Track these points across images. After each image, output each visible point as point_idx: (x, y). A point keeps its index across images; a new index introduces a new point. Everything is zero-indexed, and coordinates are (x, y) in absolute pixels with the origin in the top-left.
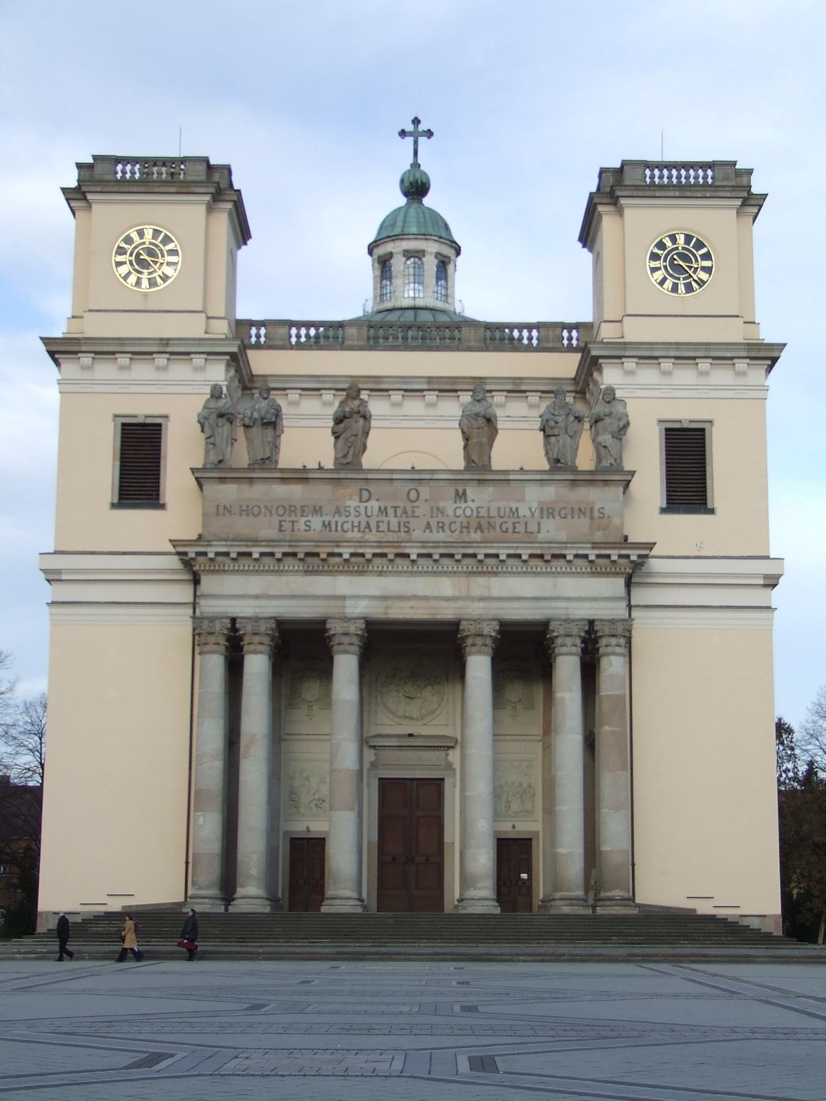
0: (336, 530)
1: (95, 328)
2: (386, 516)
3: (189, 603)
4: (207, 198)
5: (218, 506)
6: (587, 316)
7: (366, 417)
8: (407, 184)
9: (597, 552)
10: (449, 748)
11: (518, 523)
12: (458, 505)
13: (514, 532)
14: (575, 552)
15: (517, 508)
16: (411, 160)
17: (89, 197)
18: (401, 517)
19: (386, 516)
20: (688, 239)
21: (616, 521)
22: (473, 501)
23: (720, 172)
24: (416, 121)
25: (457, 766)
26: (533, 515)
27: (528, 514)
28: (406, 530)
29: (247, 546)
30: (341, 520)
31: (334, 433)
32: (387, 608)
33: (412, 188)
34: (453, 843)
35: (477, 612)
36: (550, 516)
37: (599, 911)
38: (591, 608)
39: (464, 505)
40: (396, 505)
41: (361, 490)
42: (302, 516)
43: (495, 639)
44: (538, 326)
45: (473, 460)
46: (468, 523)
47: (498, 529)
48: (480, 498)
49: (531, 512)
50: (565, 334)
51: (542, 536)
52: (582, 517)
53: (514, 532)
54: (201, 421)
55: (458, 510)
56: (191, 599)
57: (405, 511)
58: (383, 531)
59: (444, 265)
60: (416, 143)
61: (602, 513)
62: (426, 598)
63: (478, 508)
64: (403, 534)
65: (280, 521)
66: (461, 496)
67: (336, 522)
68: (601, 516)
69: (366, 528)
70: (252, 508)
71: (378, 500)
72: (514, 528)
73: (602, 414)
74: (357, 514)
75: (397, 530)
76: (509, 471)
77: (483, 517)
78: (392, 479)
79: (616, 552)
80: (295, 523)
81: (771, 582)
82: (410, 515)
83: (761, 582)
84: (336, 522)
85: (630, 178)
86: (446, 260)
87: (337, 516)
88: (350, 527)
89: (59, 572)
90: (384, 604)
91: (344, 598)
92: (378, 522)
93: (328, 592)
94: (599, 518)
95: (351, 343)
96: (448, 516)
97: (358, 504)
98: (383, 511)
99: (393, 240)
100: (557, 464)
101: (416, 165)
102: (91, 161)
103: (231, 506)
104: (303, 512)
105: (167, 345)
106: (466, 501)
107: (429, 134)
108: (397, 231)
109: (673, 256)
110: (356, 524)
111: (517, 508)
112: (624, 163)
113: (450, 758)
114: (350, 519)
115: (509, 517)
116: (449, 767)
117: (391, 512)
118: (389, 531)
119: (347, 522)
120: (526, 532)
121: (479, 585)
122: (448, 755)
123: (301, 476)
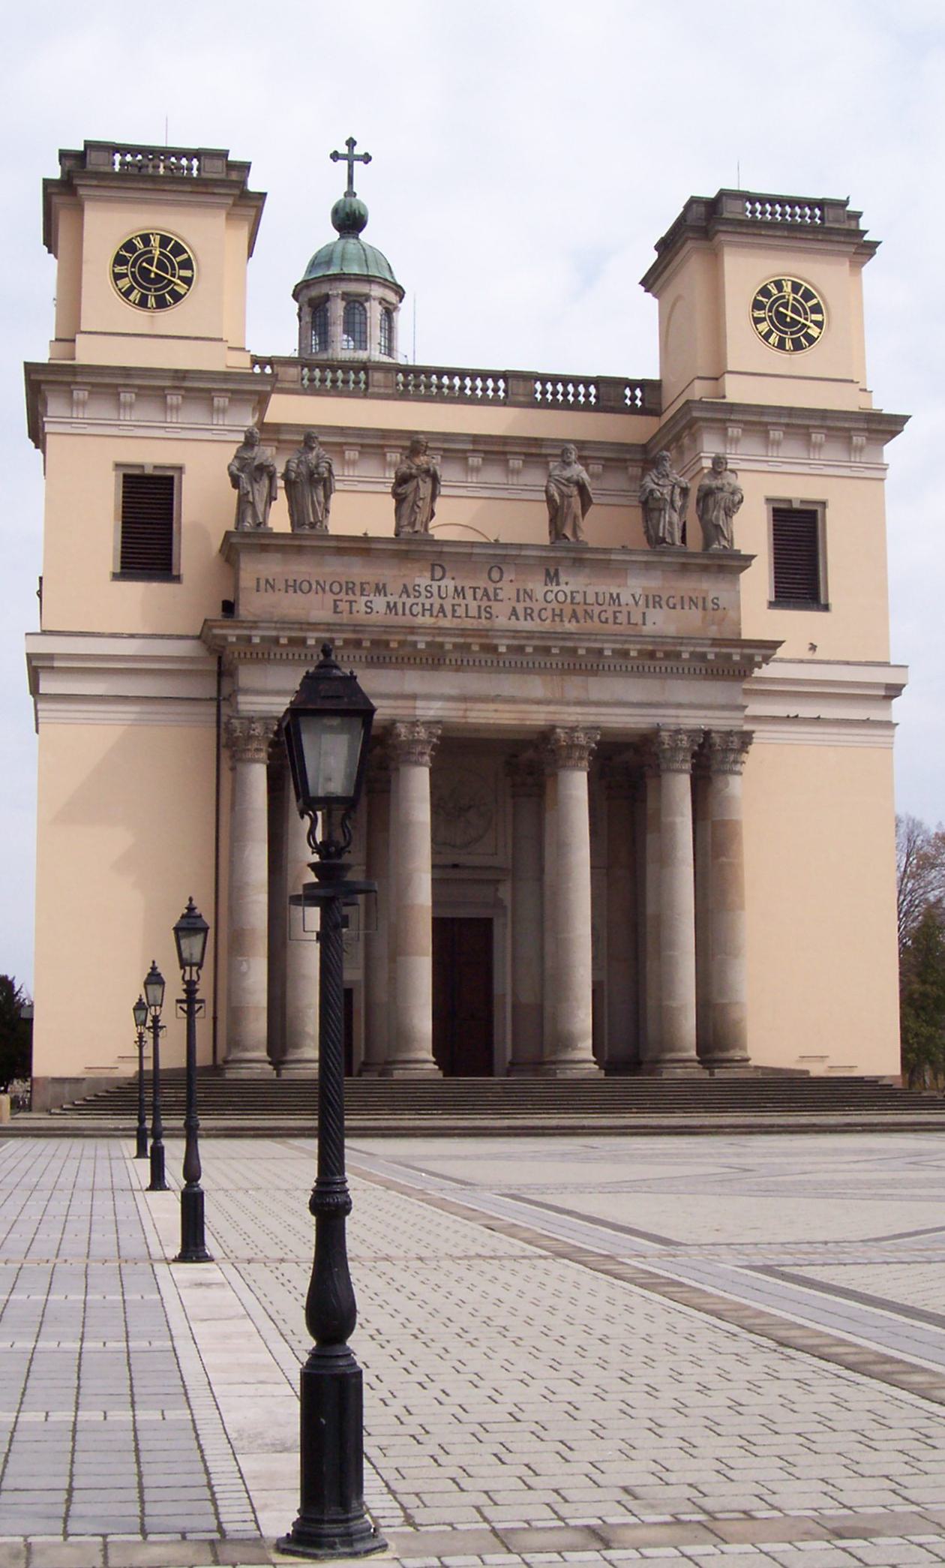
0: (404, 614)
1: (89, 353)
2: (464, 598)
3: (211, 699)
4: (230, 201)
5: (258, 579)
6: (654, 375)
7: (435, 479)
8: (342, 215)
9: (717, 650)
10: (498, 881)
11: (620, 612)
12: (549, 588)
13: (615, 623)
14: (692, 649)
15: (618, 595)
16: (346, 189)
17: (82, 191)
18: (481, 600)
19: (464, 598)
20: (796, 287)
21: (731, 614)
22: (567, 584)
23: (830, 213)
24: (351, 143)
25: (508, 903)
26: (637, 603)
27: (631, 601)
28: (488, 615)
29: (301, 629)
30: (409, 601)
31: (395, 494)
32: (466, 710)
33: (349, 220)
34: (504, 995)
35: (573, 718)
36: (657, 605)
37: (719, 1074)
38: (706, 717)
39: (556, 589)
40: (474, 585)
41: (433, 565)
42: (362, 595)
43: (592, 752)
44: (598, 381)
45: (564, 535)
46: (561, 610)
47: (596, 619)
48: (572, 583)
49: (634, 598)
50: (628, 392)
51: (648, 629)
52: (693, 607)
53: (615, 623)
54: (236, 472)
55: (550, 593)
56: (214, 694)
57: (486, 593)
58: (459, 617)
59: (389, 312)
60: (351, 167)
61: (716, 604)
62: (512, 700)
63: (572, 593)
64: (483, 621)
65: (335, 601)
66: (552, 577)
67: (404, 604)
68: (716, 607)
69: (439, 612)
70: (301, 583)
71: (453, 579)
72: (615, 618)
73: (714, 486)
74: (429, 595)
75: (477, 616)
76: (611, 549)
77: (579, 604)
78: (471, 554)
79: (738, 650)
80: (354, 604)
81: (893, 691)
82: (492, 597)
83: (882, 693)
84: (404, 604)
85: (730, 210)
86: (391, 307)
87: (404, 596)
88: (421, 611)
89: (51, 657)
90: (463, 706)
91: (414, 697)
92: (453, 606)
93: (395, 689)
94: (713, 609)
95: (376, 390)
96: (537, 600)
97: (429, 582)
98: (459, 592)
99: (330, 280)
100: (655, 541)
101: (350, 193)
102: (81, 148)
103: (274, 580)
104: (362, 590)
105: (184, 378)
106: (558, 584)
107: (367, 158)
108: (334, 270)
109: (778, 307)
110: (427, 607)
111: (618, 595)
112: (723, 194)
113: (500, 895)
114: (421, 600)
115: (610, 605)
116: (498, 904)
117: (469, 593)
118: (467, 617)
119: (417, 604)
120: (629, 623)
121: (574, 686)
122: (497, 890)
123: (361, 547)
